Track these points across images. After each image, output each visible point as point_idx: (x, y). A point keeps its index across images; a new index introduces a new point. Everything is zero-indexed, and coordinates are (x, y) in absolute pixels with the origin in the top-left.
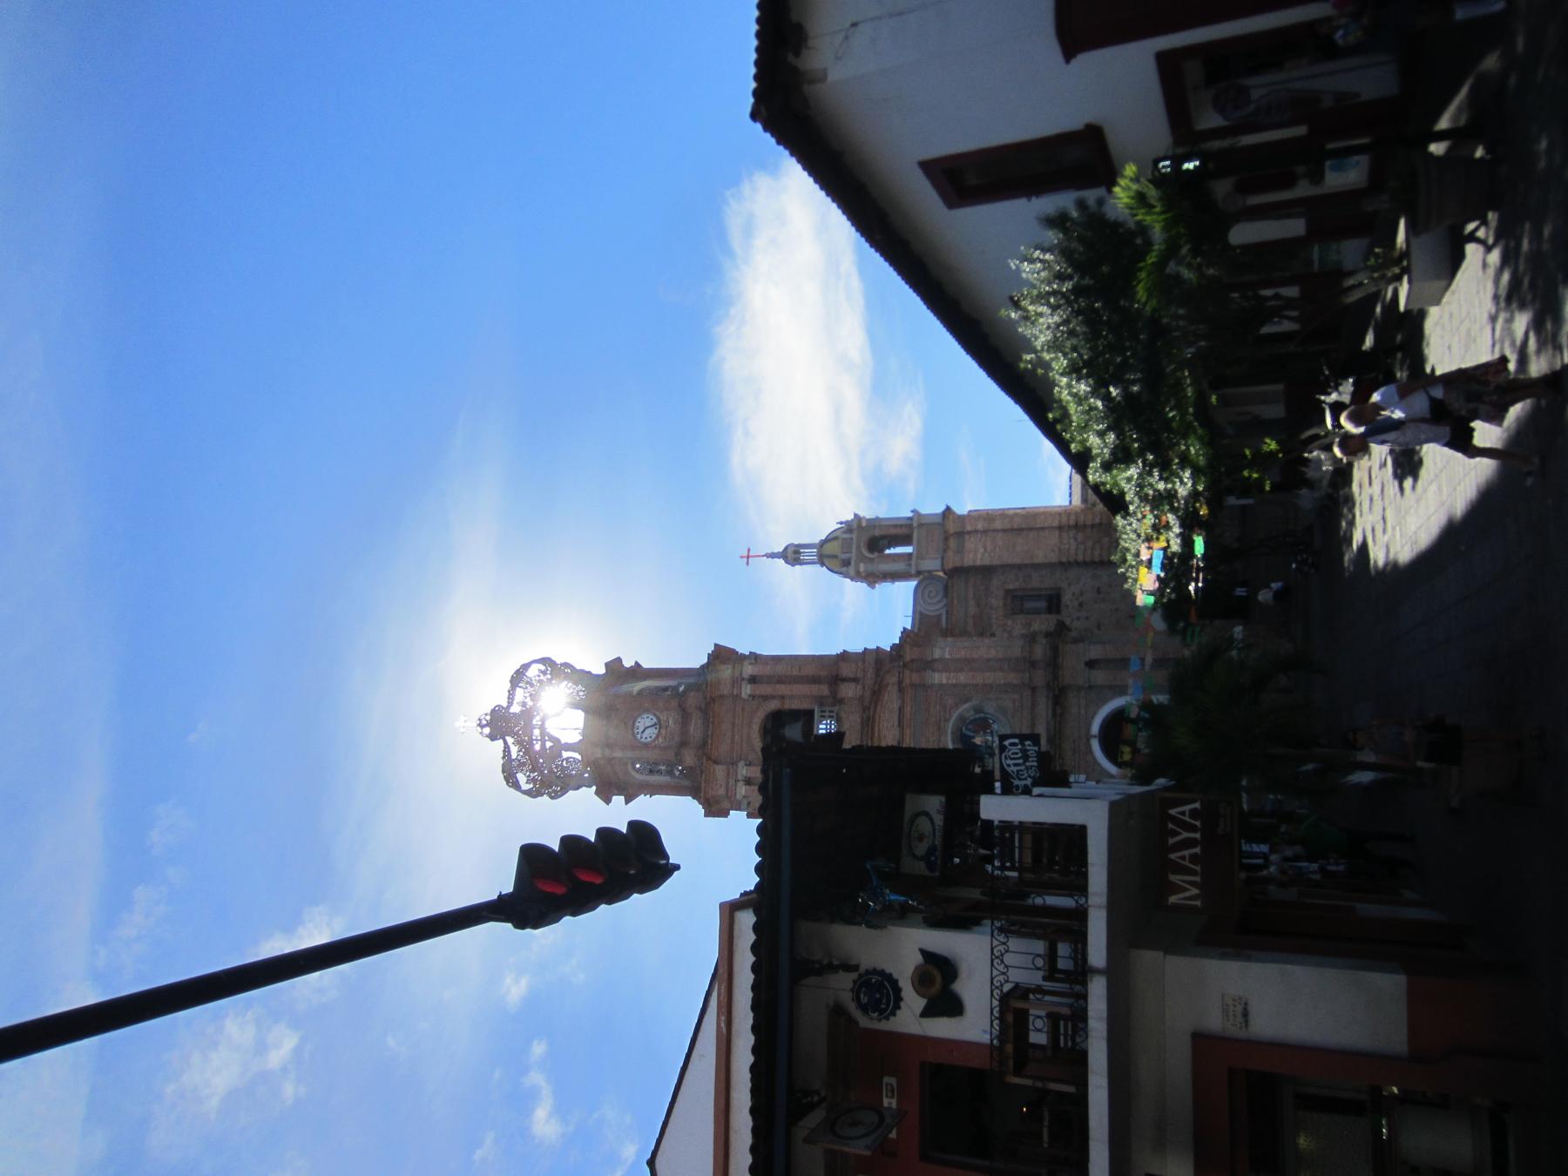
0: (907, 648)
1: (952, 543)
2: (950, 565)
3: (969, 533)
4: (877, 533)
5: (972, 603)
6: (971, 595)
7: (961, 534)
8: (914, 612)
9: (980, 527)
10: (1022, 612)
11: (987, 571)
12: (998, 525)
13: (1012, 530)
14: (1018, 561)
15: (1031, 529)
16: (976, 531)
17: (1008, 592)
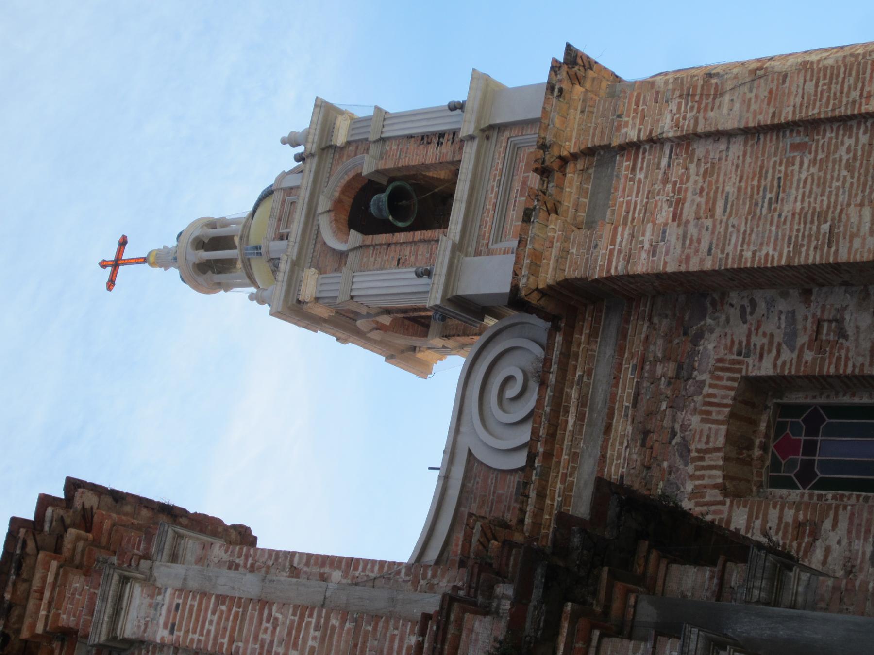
0: (45, 571)
1: (572, 187)
2: (548, 277)
3: (631, 148)
4: (368, 165)
5: (623, 427)
6: (625, 394)
7: (600, 156)
8: (451, 453)
9: (666, 127)
10: (806, 477)
11: (687, 297)
12: (728, 114)
13: (777, 129)
14: (772, 252)
15: (844, 121)
16: (655, 142)
17: (756, 390)
